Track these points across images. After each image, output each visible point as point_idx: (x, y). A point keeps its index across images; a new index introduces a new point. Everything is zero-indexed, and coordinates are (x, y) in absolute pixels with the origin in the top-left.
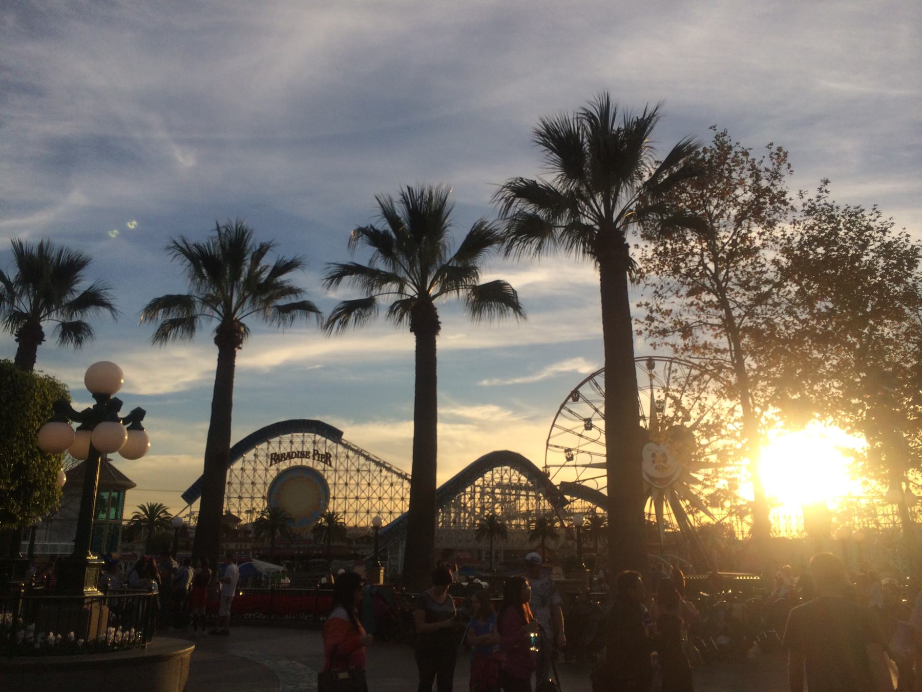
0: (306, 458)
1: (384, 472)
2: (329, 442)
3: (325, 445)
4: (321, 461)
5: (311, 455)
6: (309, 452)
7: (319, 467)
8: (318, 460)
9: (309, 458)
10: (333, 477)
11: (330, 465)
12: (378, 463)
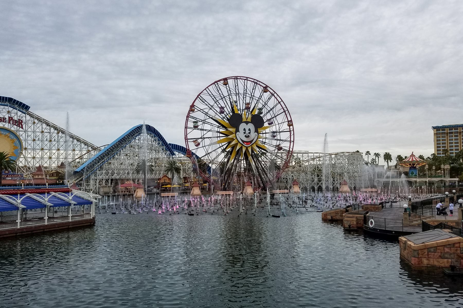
0: (3, 122)
1: (60, 134)
2: (19, 113)
3: (17, 114)
4: (15, 125)
5: (7, 119)
6: (6, 118)
7: (14, 128)
8: (13, 124)
9: (5, 122)
10: (24, 135)
11: (22, 128)
12: (56, 128)
